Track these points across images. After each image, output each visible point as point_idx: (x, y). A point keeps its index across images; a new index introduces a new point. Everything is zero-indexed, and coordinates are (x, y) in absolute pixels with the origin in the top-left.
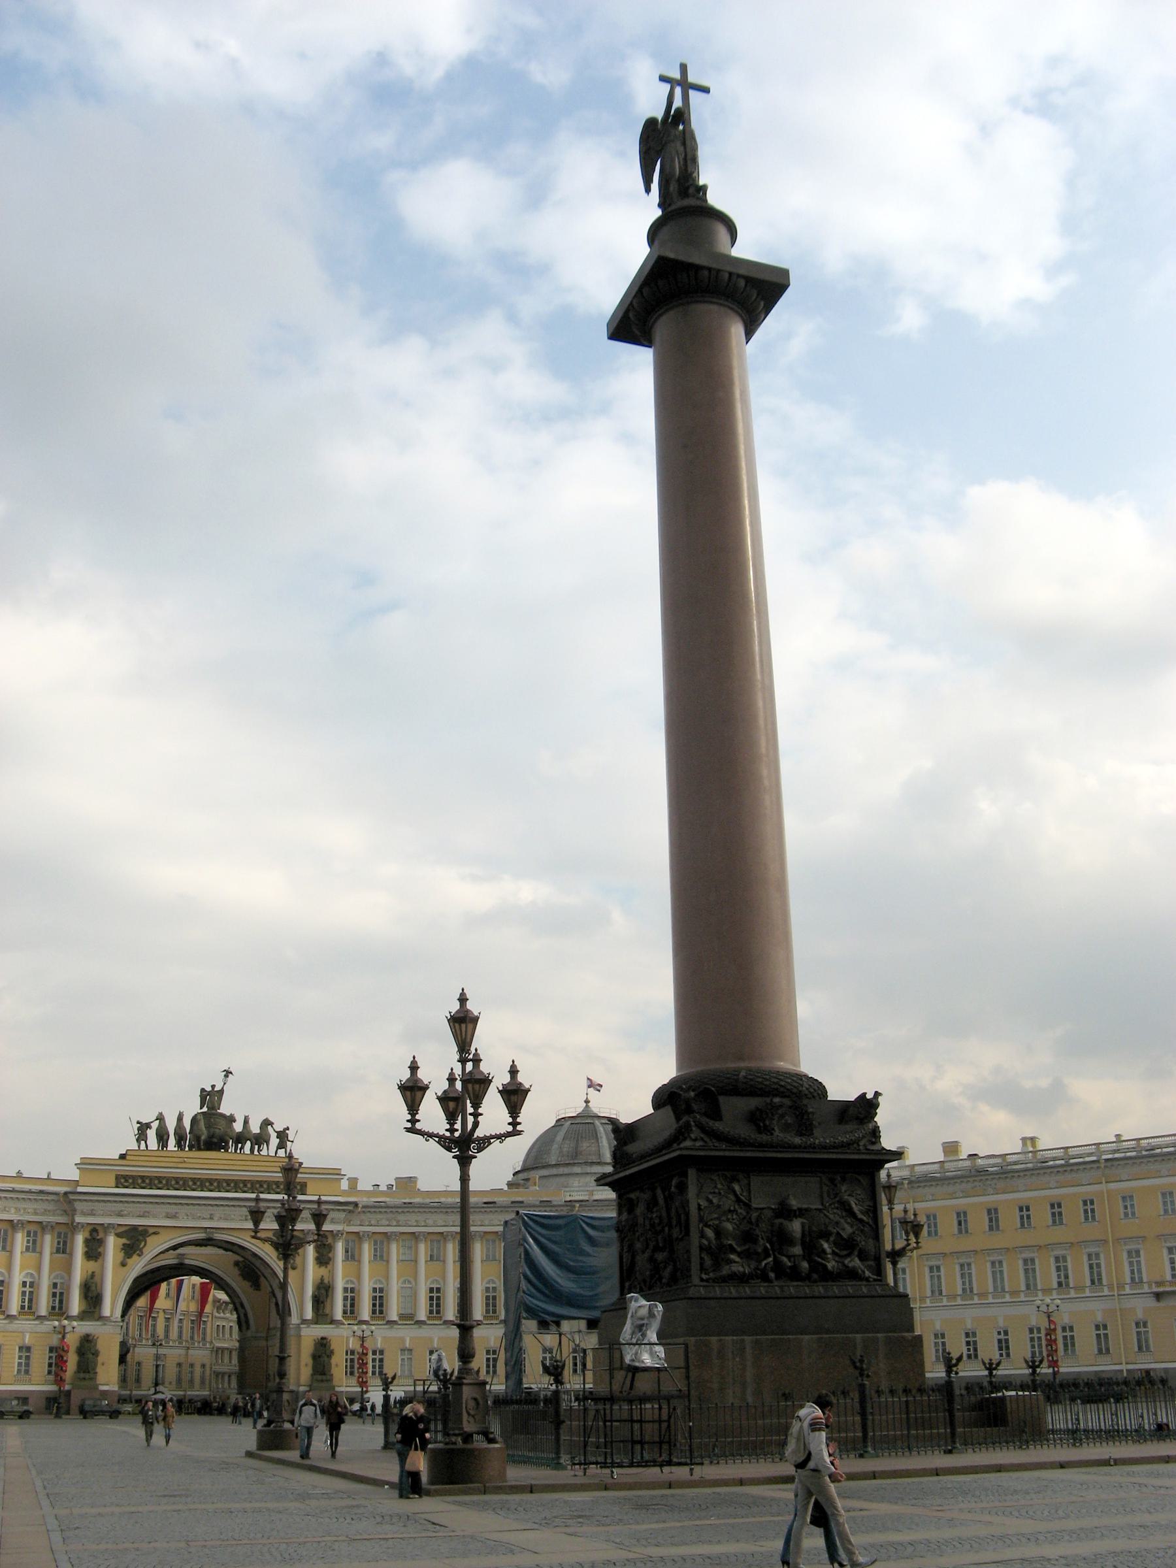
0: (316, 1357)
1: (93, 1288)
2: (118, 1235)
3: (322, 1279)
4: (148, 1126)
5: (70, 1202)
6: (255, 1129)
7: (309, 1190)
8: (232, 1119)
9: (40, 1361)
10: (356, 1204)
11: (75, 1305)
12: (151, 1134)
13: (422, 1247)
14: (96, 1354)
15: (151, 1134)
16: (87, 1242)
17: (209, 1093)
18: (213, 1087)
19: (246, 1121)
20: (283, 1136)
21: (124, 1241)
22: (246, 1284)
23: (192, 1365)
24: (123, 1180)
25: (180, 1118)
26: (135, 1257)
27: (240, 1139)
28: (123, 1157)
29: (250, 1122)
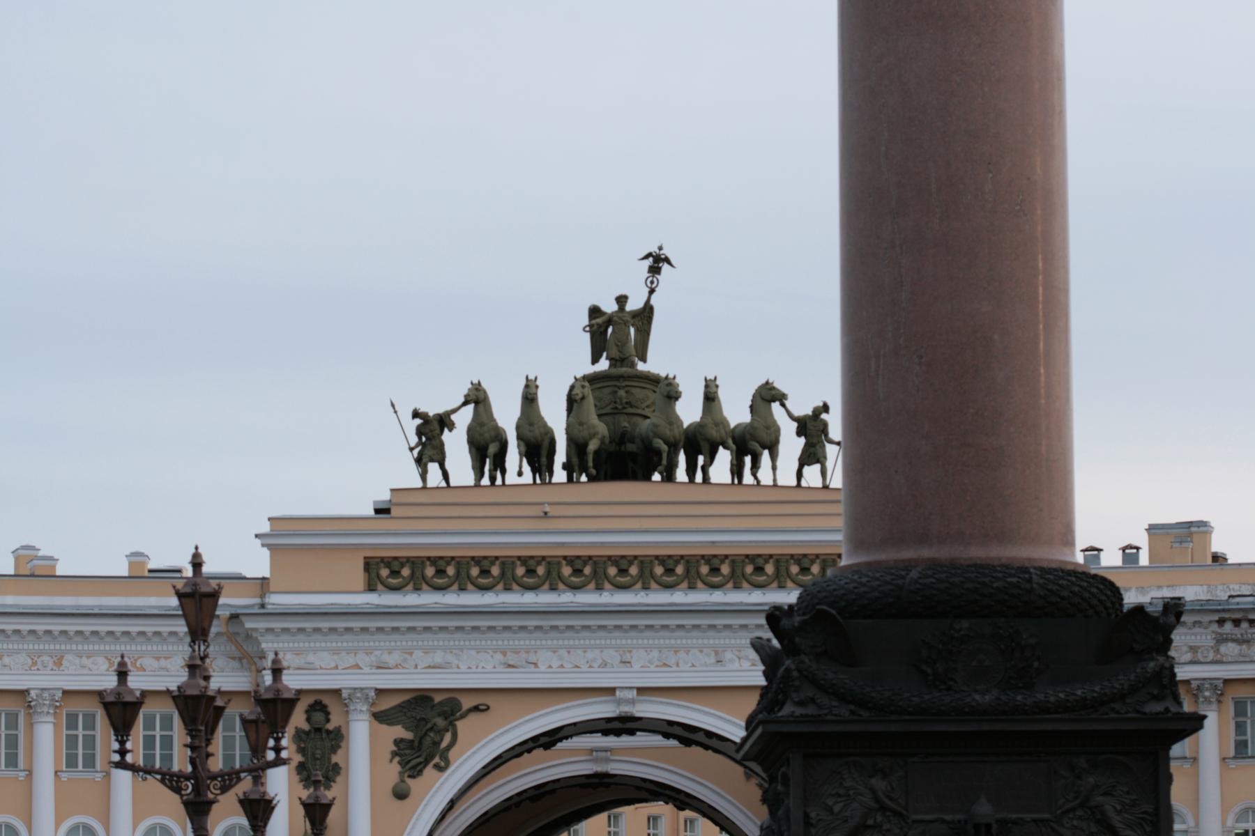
2: (381, 717)
4: (444, 422)
5: (249, 636)
6: (736, 412)
12: (456, 444)
15: (456, 444)
17: (610, 321)
18: (622, 300)
19: (710, 398)
21: (399, 732)
24: (384, 570)
25: (529, 398)
26: (429, 771)
27: (699, 443)
28: (381, 511)
29: (722, 394)
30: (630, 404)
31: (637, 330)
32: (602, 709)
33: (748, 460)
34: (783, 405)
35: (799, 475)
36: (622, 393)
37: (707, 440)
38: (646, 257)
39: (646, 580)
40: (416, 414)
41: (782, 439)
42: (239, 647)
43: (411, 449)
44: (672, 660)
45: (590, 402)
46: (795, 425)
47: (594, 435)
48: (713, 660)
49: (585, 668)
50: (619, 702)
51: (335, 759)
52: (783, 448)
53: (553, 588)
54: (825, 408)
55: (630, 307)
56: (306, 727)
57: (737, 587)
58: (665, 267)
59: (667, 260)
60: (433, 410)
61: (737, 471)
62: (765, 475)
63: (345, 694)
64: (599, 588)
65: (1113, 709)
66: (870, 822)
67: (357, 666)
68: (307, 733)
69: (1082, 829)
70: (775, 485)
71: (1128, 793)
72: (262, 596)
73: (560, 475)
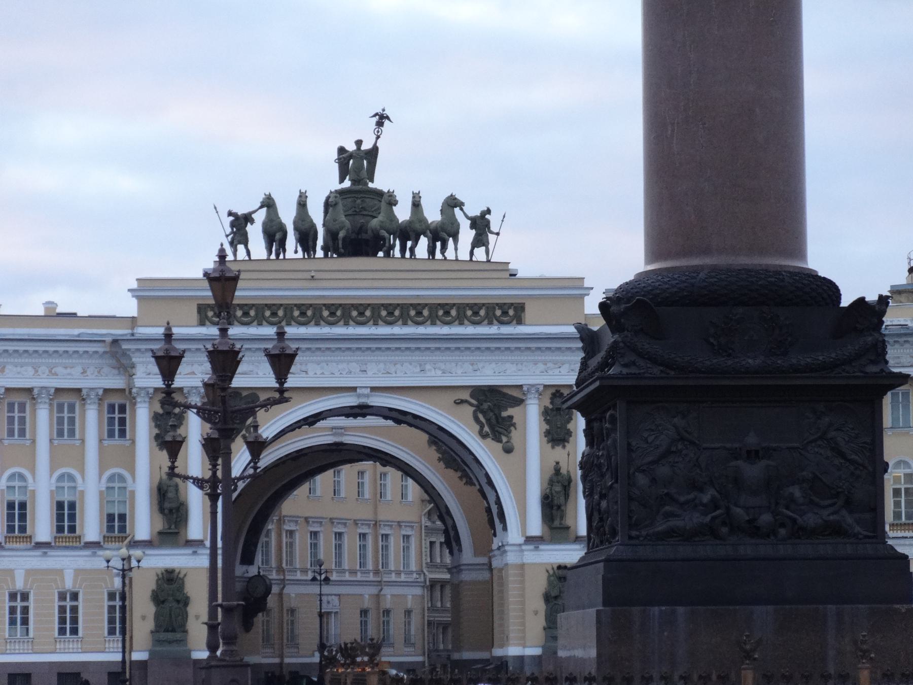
1: (170, 495)
3: (557, 471)
4: (247, 218)
5: (125, 354)
6: (433, 214)
8: (391, 201)
9: (93, 614)
11: (143, 523)
12: (255, 232)
14: (185, 602)
15: (255, 232)
16: (157, 419)
17: (351, 156)
18: (359, 143)
19: (416, 205)
20: (481, 225)
22: (454, 475)
23: (387, 612)
25: (302, 204)
27: (408, 234)
29: (423, 202)
30: (364, 209)
31: (368, 163)
32: (349, 401)
33: (438, 244)
34: (462, 209)
35: (472, 253)
36: (359, 201)
37: (414, 231)
39: (376, 319)
40: (230, 214)
42: (118, 361)
43: (227, 236)
44: (393, 370)
45: (340, 207)
46: (469, 222)
47: (341, 228)
48: (418, 369)
49: (337, 374)
51: (181, 431)
52: (461, 236)
53: (317, 324)
54: (488, 211)
56: (161, 411)
57: (433, 324)
58: (386, 122)
59: (388, 118)
60: (241, 211)
61: (432, 251)
62: (450, 254)
63: (185, 391)
64: (346, 324)
65: (844, 370)
66: (674, 449)
67: (193, 373)
68: (162, 415)
69: (821, 454)
70: (457, 260)
71: (853, 429)
72: (133, 328)
73: (320, 253)
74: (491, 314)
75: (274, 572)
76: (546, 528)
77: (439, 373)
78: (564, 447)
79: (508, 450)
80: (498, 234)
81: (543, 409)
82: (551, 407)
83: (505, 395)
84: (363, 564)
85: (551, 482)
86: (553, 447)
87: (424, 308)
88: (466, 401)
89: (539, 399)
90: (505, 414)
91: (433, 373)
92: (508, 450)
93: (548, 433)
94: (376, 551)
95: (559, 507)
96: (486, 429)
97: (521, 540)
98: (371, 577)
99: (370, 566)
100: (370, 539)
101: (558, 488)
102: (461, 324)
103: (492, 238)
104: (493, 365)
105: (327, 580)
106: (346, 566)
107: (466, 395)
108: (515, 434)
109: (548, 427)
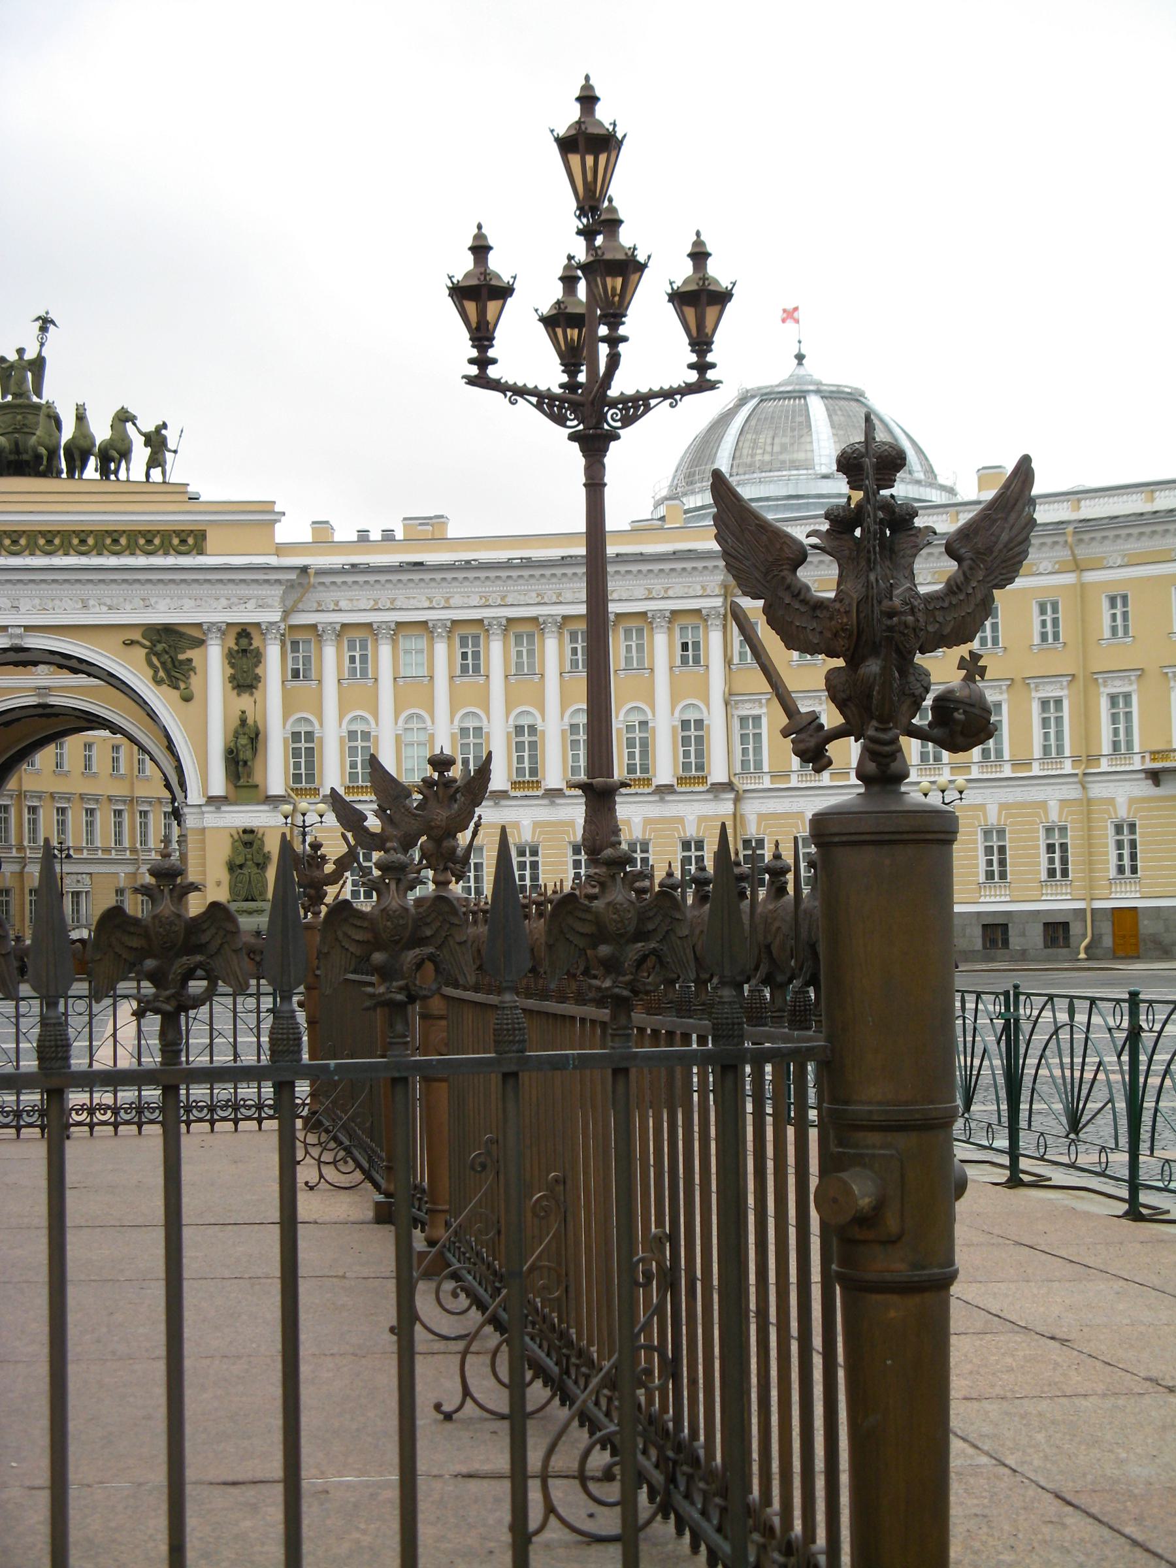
0: (232, 867)
3: (243, 722)
6: (101, 432)
7: (210, 543)
10: (304, 570)
13: (441, 648)
18: (21, 351)
19: (81, 418)
20: (157, 442)
29: (89, 415)
31: (33, 375)
34: (134, 424)
35: (148, 475)
36: (19, 417)
38: (39, 318)
41: (134, 448)
44: (50, 605)
48: (80, 605)
50: (11, 636)
52: (134, 455)
54: (165, 426)
55: (27, 357)
58: (51, 327)
59: (52, 322)
62: (122, 475)
70: (128, 481)
74: (166, 543)
75: (14, 850)
76: (231, 787)
77: (104, 609)
78: (252, 694)
79: (187, 699)
80: (175, 452)
81: (226, 651)
82: (236, 648)
83: (182, 635)
84: (119, 841)
85: (237, 735)
86: (239, 695)
87: (88, 536)
88: (138, 642)
89: (223, 639)
90: (181, 657)
91: (97, 610)
92: (187, 699)
93: (232, 678)
94: (132, 828)
95: (245, 763)
96: (161, 674)
97: (202, 801)
98: (128, 855)
99: (126, 844)
100: (126, 815)
101: (243, 741)
102: (133, 554)
103: (169, 456)
104: (168, 600)
105: (68, 856)
106: (98, 843)
107: (137, 636)
108: (194, 680)
109: (232, 671)
